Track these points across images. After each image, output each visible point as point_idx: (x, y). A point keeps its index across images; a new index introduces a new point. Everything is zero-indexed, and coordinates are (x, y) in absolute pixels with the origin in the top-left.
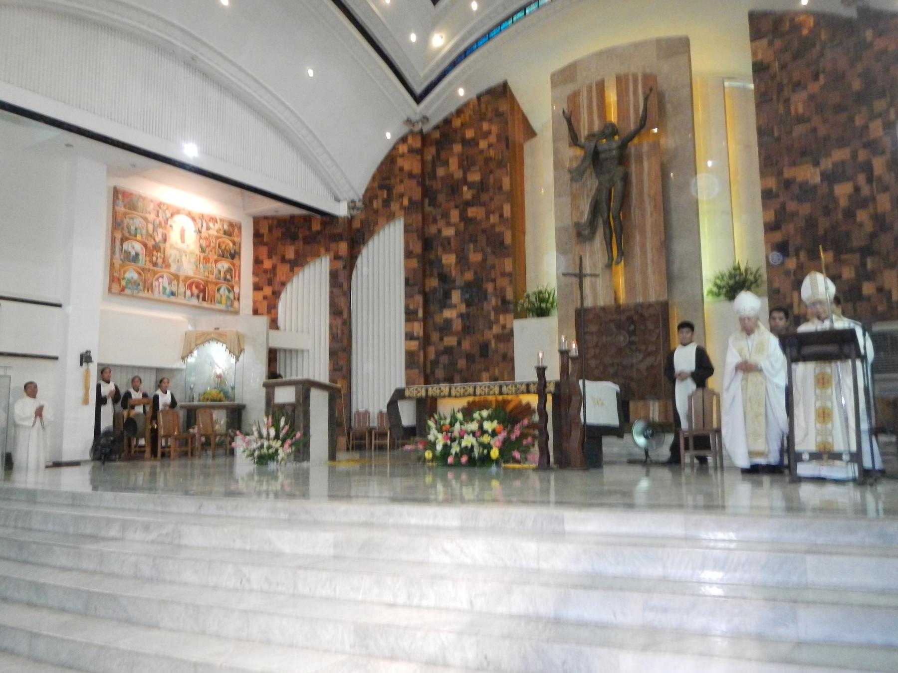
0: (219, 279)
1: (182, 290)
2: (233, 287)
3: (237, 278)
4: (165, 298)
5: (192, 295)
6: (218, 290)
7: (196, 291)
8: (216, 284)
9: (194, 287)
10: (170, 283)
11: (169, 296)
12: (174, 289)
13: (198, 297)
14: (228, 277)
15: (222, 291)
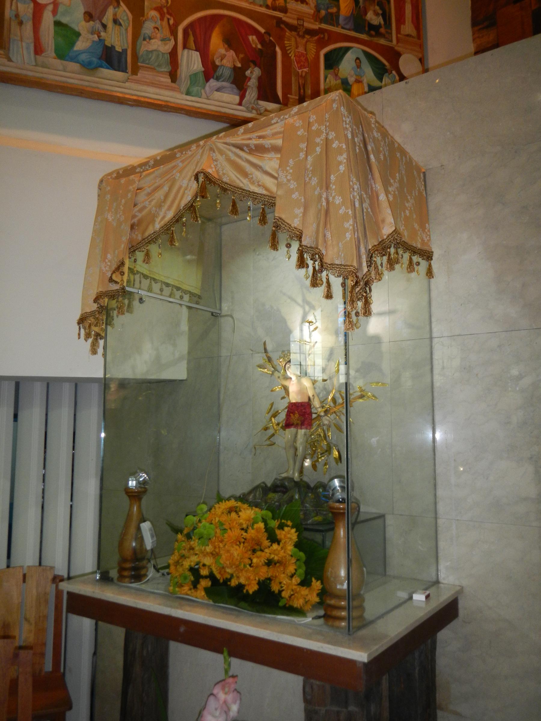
0: (332, 19)
1: (158, 46)
2: (394, 56)
3: (408, 28)
4: (70, 73)
5: (210, 71)
6: (333, 61)
7: (227, 58)
8: (322, 38)
9: (216, 41)
10: (89, 16)
11: (89, 67)
12: (118, 39)
13: (239, 81)
14: (373, 17)
15: (346, 66)
